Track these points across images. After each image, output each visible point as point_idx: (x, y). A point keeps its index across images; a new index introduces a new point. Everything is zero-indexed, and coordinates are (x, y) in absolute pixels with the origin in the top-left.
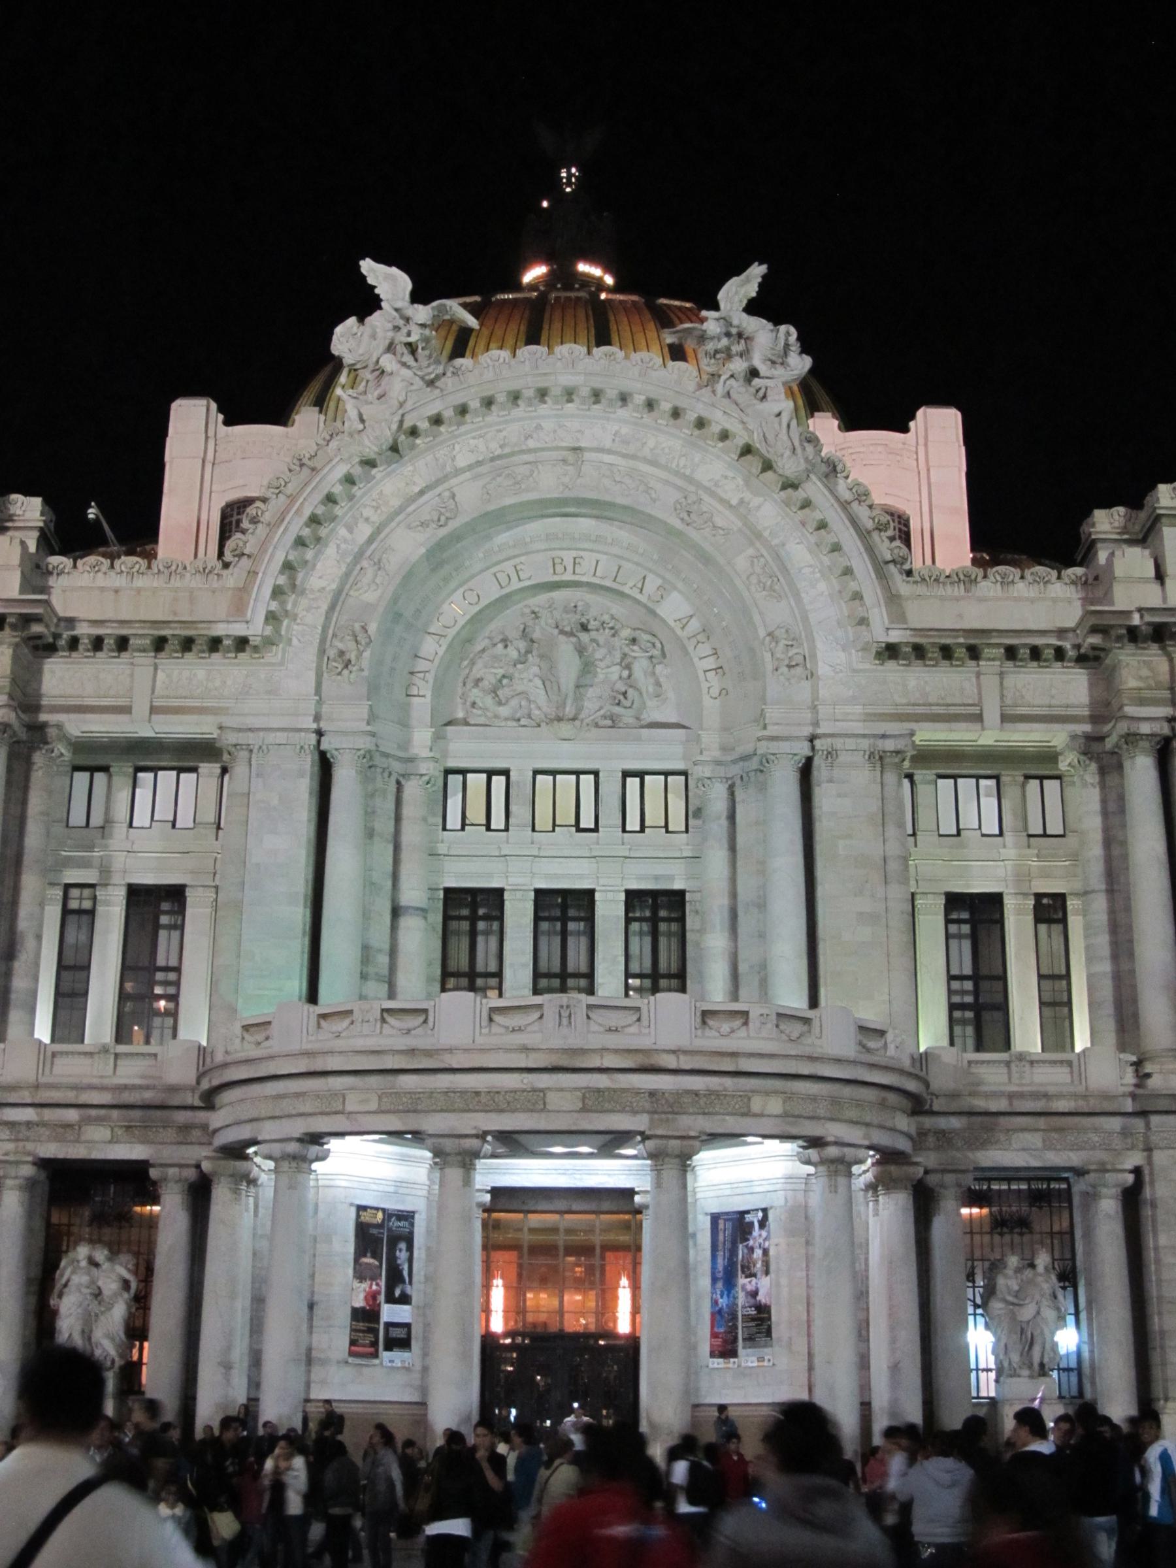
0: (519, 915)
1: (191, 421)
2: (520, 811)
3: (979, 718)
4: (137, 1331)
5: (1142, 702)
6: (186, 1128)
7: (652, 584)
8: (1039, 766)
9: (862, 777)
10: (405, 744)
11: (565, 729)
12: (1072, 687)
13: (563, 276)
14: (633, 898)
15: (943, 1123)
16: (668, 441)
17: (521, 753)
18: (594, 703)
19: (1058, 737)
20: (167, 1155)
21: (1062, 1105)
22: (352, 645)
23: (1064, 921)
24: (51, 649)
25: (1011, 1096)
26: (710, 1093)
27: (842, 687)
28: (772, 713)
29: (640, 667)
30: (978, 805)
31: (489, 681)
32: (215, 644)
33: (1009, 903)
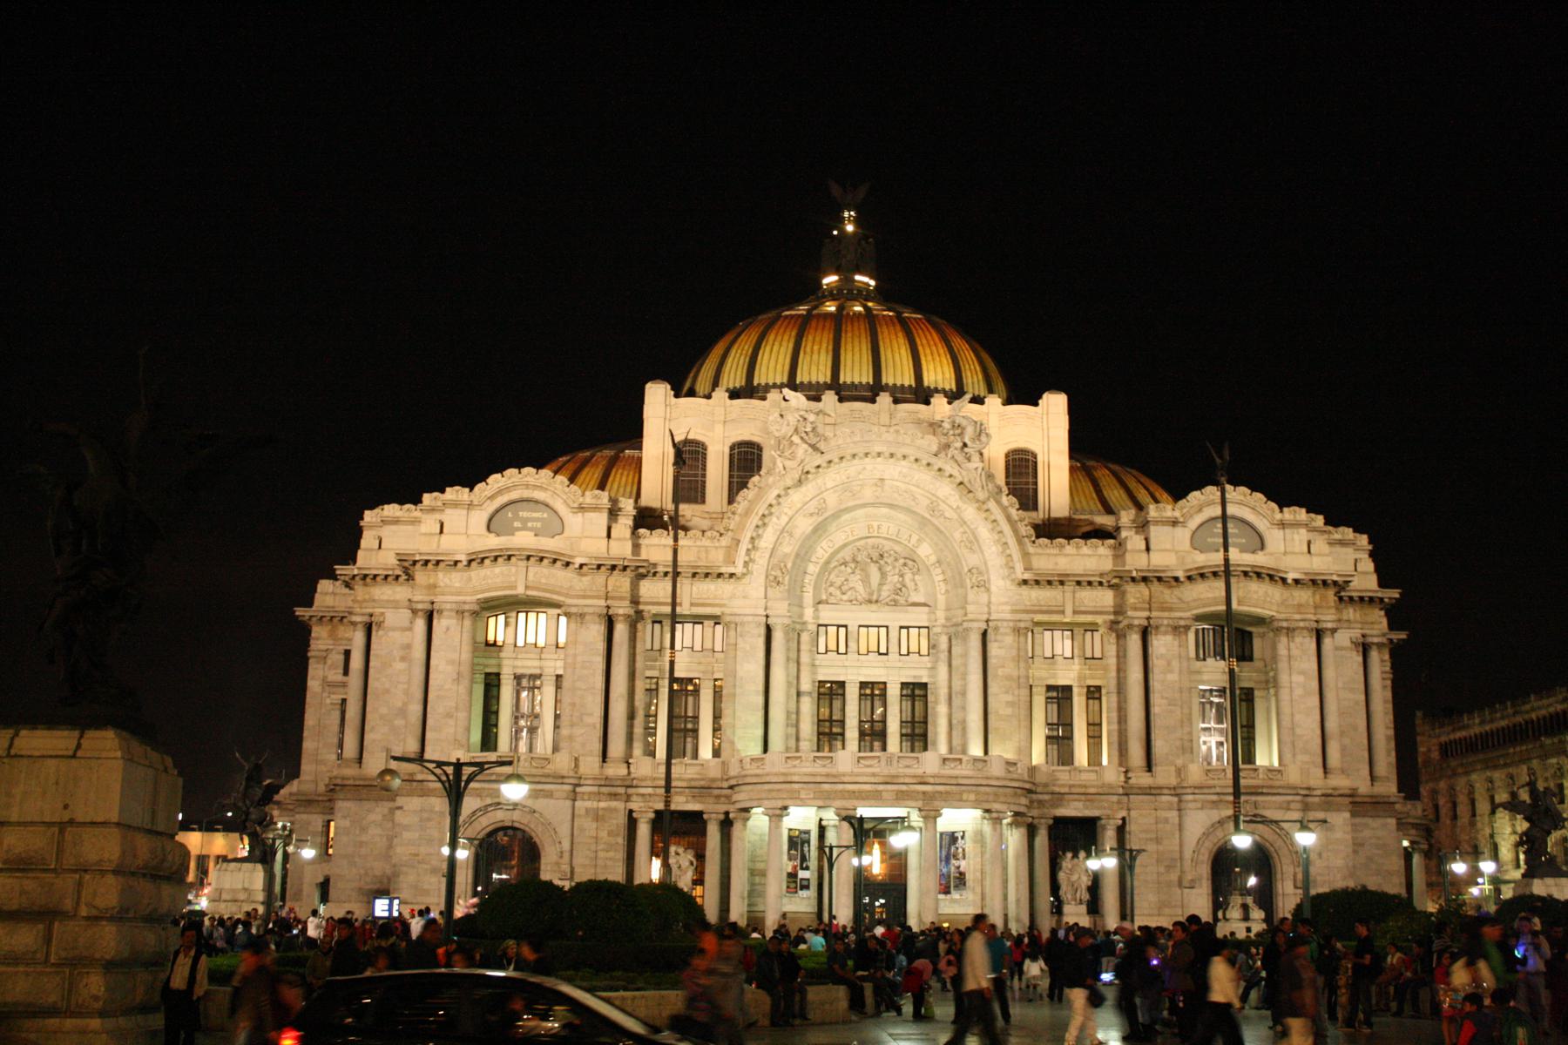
0: (852, 693)
1: (656, 395)
2: (852, 645)
3: (1063, 612)
4: (699, 881)
5: (1136, 609)
6: (718, 797)
7: (915, 538)
8: (1091, 628)
9: (1009, 639)
10: (801, 616)
11: (874, 607)
12: (1106, 598)
13: (847, 280)
14: (904, 685)
15: (1041, 797)
16: (924, 477)
17: (853, 617)
18: (885, 593)
19: (1099, 619)
20: (713, 810)
21: (1092, 790)
22: (778, 573)
23: (1100, 699)
24: (643, 576)
25: (1071, 786)
26: (947, 793)
27: (1001, 596)
28: (970, 608)
29: (908, 577)
30: (1063, 644)
31: (838, 582)
32: (720, 575)
33: (1075, 690)
